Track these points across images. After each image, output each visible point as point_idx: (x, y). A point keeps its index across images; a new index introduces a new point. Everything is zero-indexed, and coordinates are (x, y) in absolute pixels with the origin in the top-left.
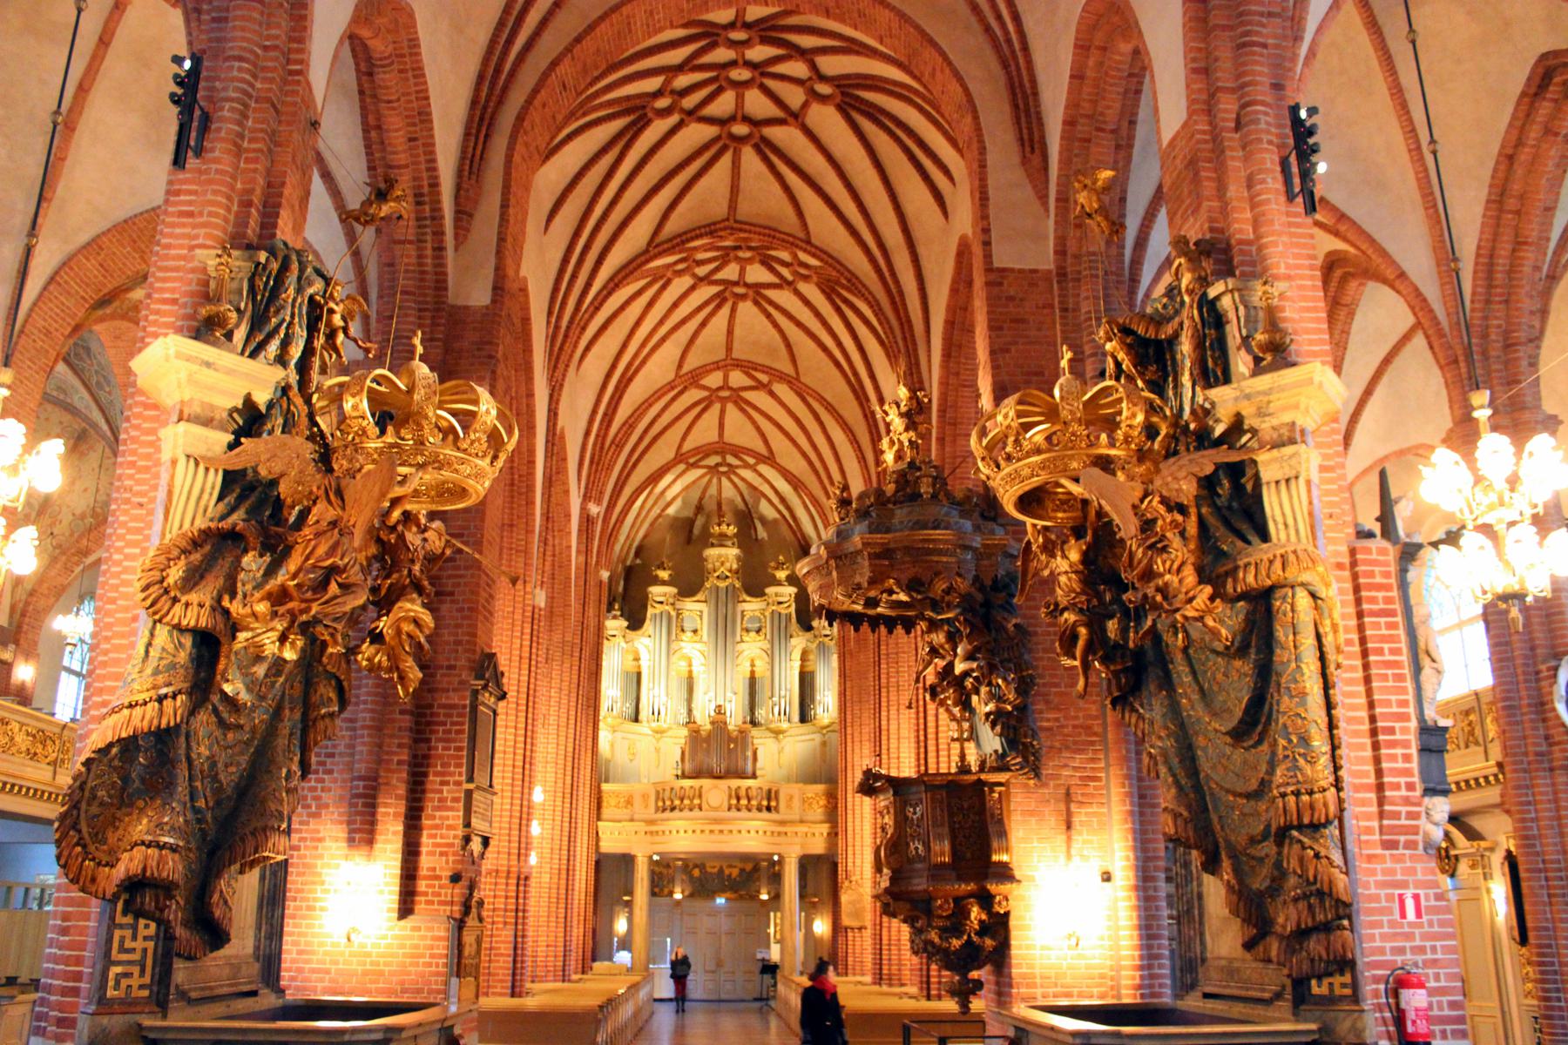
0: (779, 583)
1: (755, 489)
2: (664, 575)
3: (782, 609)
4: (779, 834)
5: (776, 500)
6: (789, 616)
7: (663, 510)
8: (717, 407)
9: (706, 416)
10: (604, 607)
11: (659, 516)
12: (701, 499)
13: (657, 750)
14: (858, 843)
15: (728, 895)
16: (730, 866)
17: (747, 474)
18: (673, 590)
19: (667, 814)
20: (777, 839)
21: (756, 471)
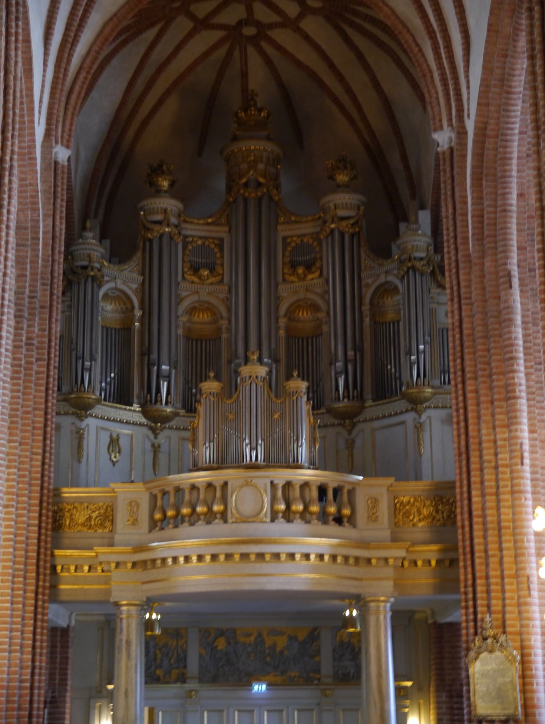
0: (339, 188)
4: (357, 559)
14: (494, 573)
19: (170, 531)
21: (298, 30)
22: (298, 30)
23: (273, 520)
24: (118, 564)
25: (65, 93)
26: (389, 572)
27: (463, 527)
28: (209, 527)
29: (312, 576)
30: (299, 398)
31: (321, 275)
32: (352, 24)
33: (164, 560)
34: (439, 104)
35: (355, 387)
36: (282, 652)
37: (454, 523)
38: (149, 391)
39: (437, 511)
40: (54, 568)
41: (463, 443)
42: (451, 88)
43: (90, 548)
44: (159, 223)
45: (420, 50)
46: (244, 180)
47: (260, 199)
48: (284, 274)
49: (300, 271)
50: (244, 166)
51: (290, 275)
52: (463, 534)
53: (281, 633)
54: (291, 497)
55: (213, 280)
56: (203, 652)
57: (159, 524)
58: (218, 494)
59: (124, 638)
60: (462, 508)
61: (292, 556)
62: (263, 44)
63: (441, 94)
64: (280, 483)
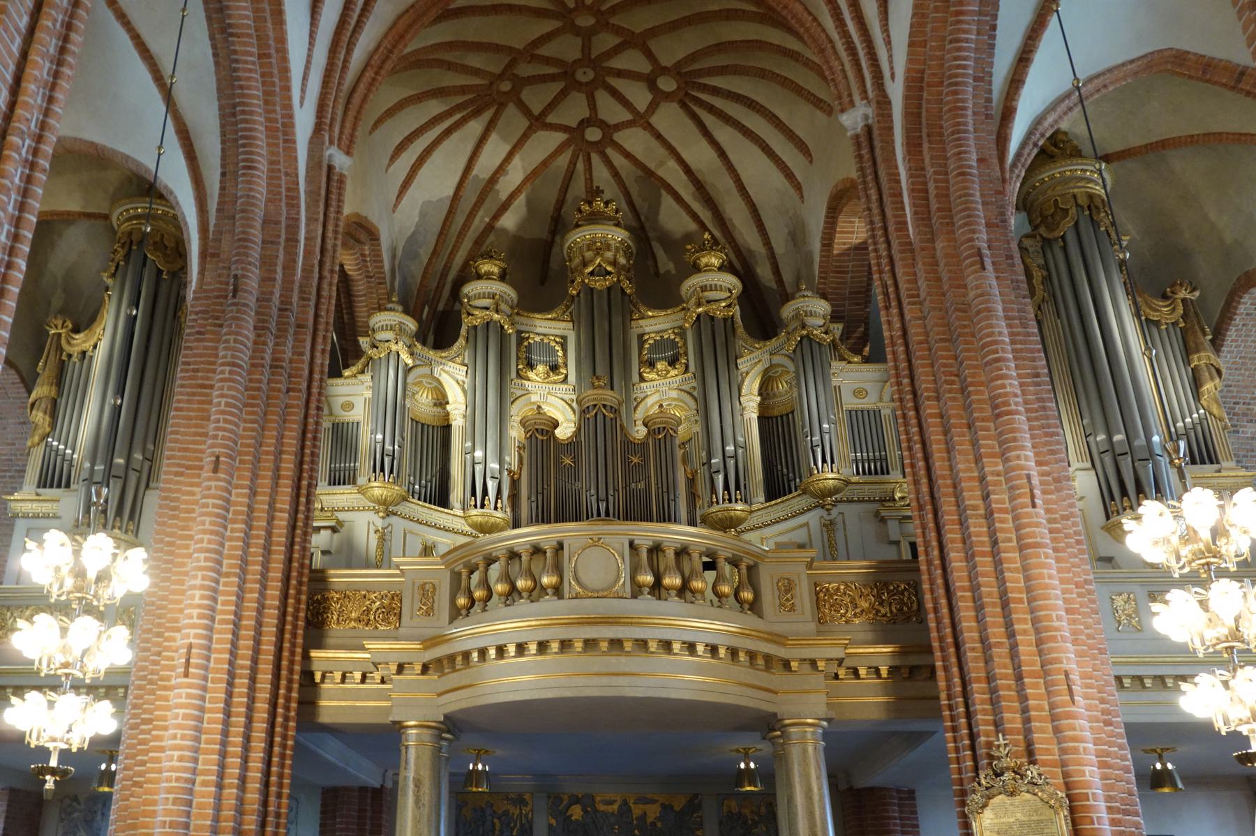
3: (719, 310)
4: (768, 658)
5: (686, 191)
6: (729, 322)
7: (496, 217)
11: (490, 228)
12: (561, 202)
16: (643, 800)
22: (649, 127)
23: (634, 596)
28: (535, 605)
29: (701, 678)
30: (668, 436)
31: (686, 370)
34: (846, 77)
39: (881, 603)
42: (862, 53)
44: (487, 309)
45: (815, 19)
46: (591, 269)
47: (609, 289)
48: (640, 374)
49: (661, 366)
50: (589, 254)
51: (649, 373)
54: (662, 568)
57: (464, 612)
61: (667, 645)
63: (848, 66)
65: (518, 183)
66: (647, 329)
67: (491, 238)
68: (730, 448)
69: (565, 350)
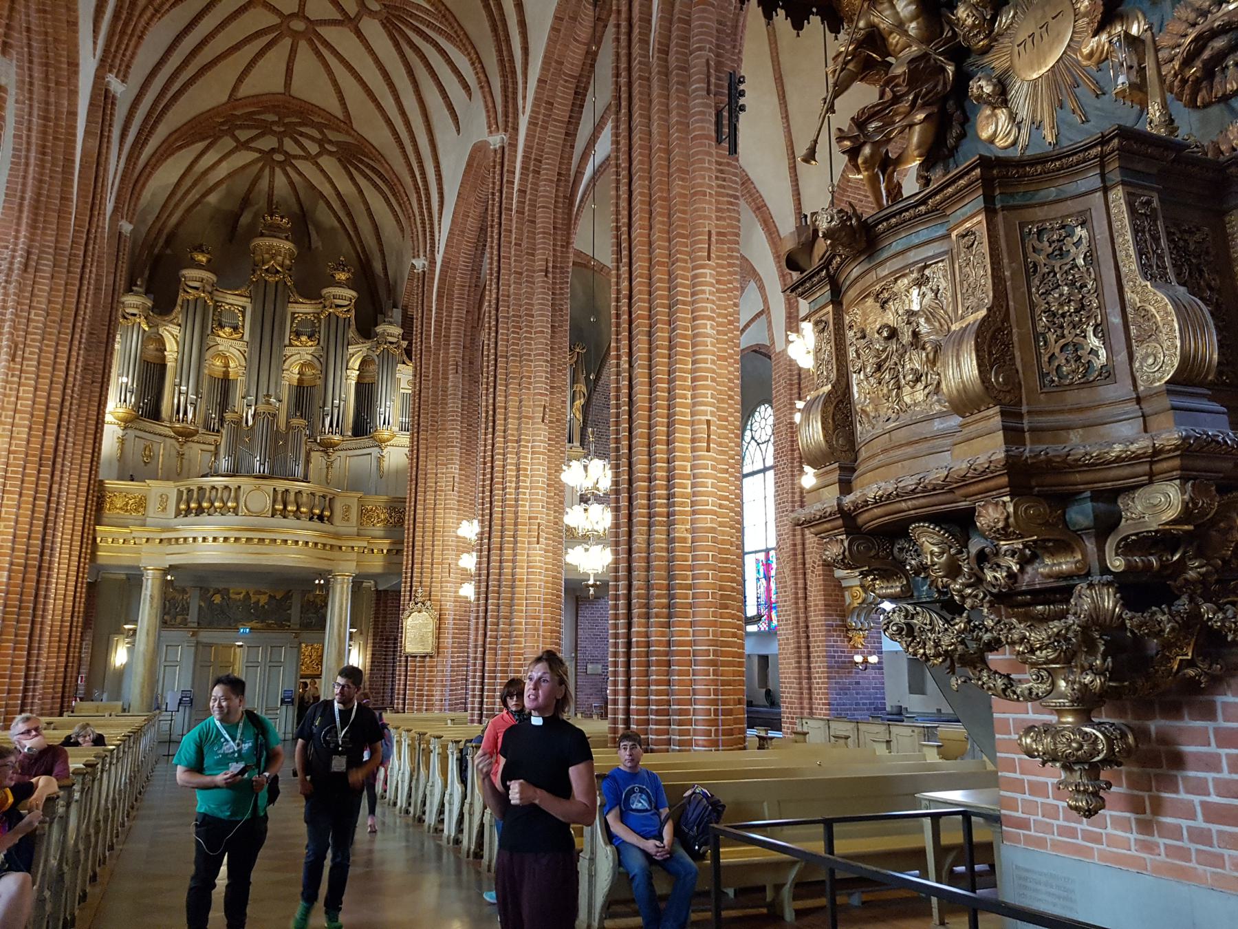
0: (339, 284)
1: (313, 187)
2: (202, 258)
3: (341, 313)
4: (332, 546)
5: (336, 205)
8: (287, 42)
9: (270, 54)
10: (122, 284)
11: (198, 202)
12: (250, 191)
13: (181, 455)
14: (427, 560)
15: (254, 624)
17: (305, 167)
18: (211, 277)
20: (329, 554)
21: (317, 164)
22: (317, 164)
23: (273, 516)
24: (148, 540)
25: (133, 181)
26: (354, 556)
27: (409, 529)
31: (318, 344)
32: (357, 168)
33: (185, 539)
35: (337, 426)
36: (263, 606)
37: (402, 525)
38: (178, 412)
40: (94, 539)
41: (414, 473)
43: (127, 527)
45: (409, 199)
47: (277, 282)
49: (304, 338)
50: (266, 256)
52: (408, 534)
53: (265, 593)
55: (235, 336)
56: (203, 604)
58: (232, 494)
59: (149, 593)
60: (409, 516)
61: (285, 541)
62: (288, 168)
64: (280, 489)
65: (222, 177)
66: (298, 310)
67: (199, 207)
68: (336, 402)
69: (244, 316)
